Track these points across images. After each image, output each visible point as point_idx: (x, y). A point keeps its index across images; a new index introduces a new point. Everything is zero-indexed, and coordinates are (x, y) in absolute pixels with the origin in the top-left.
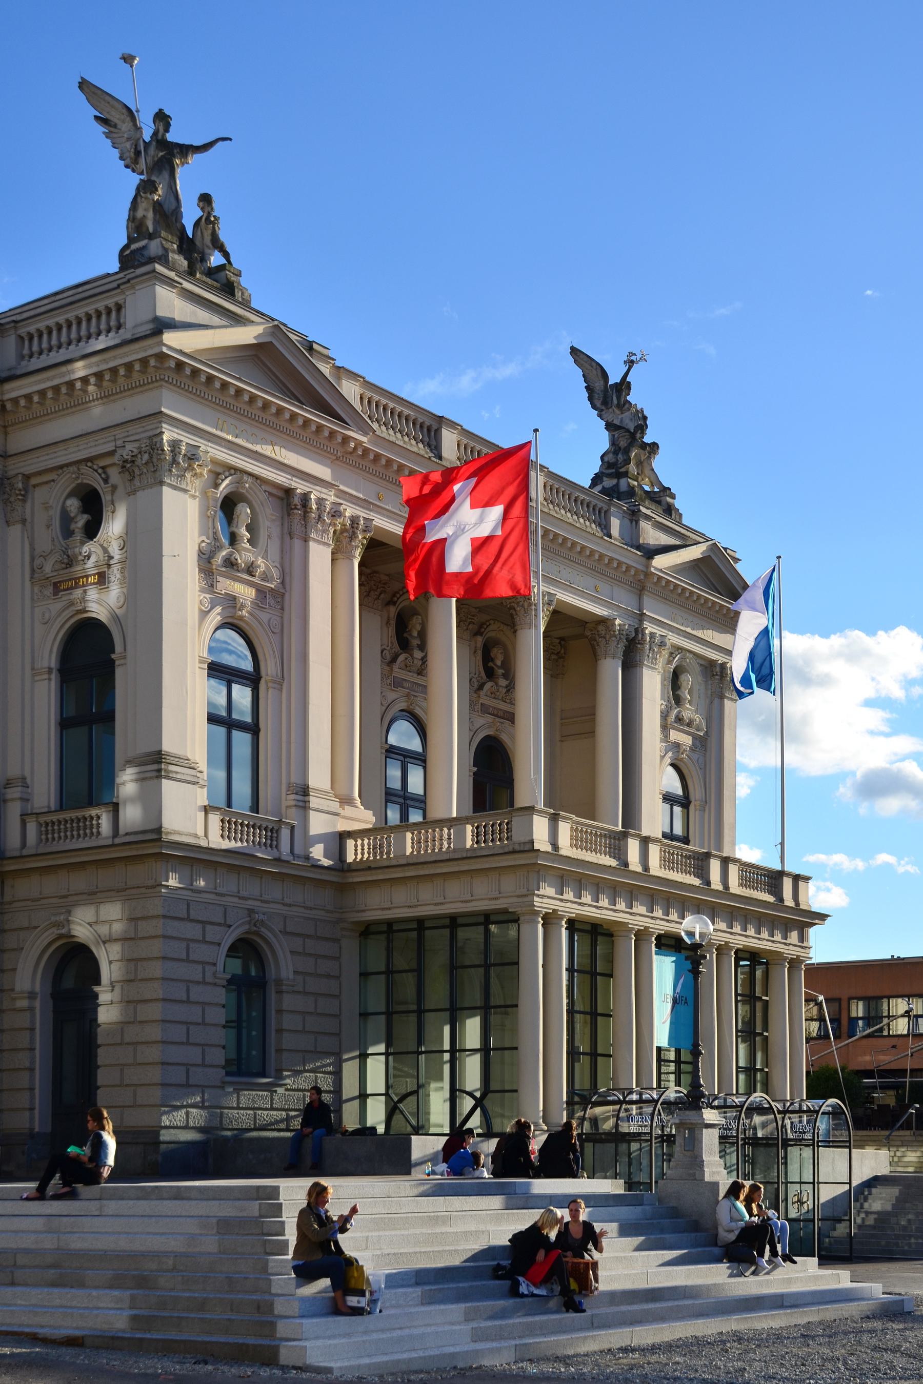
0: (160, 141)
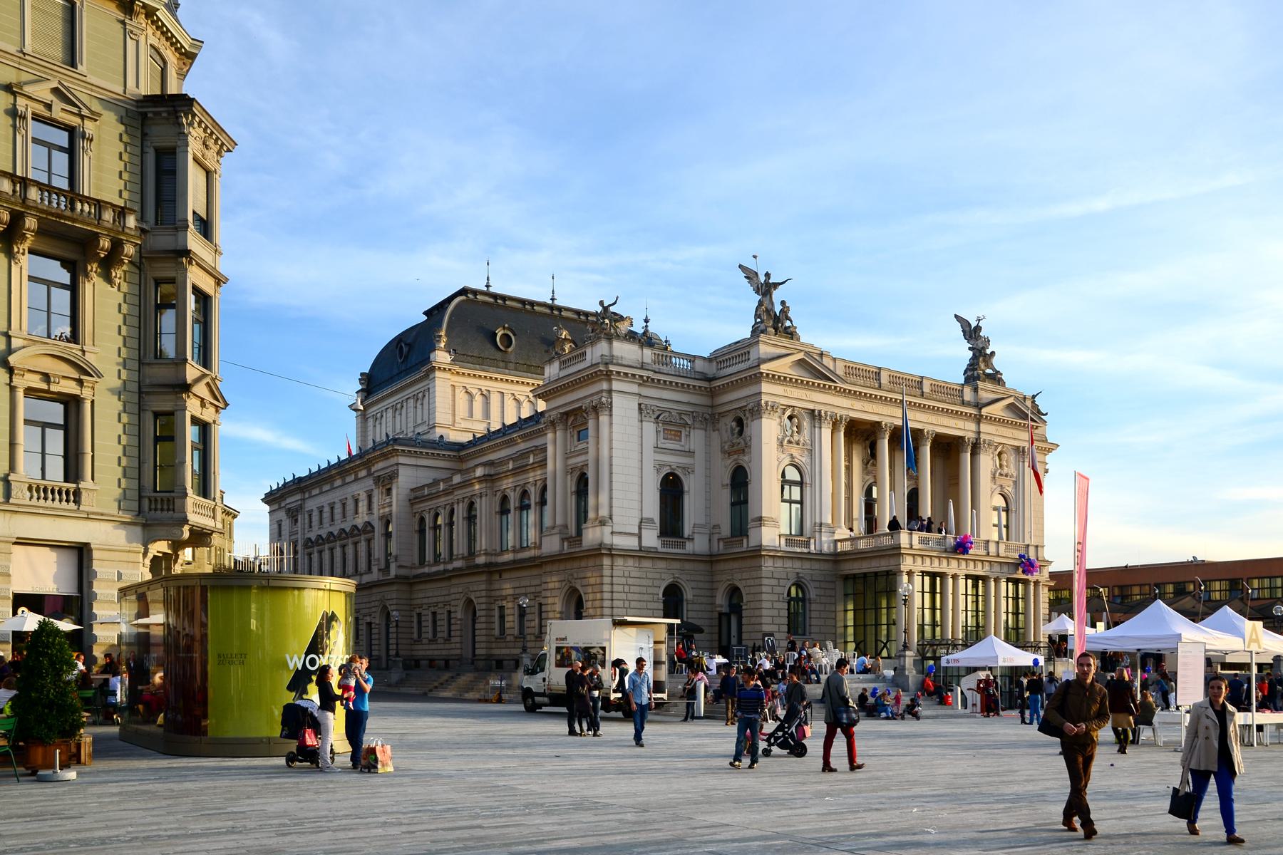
0: (767, 283)
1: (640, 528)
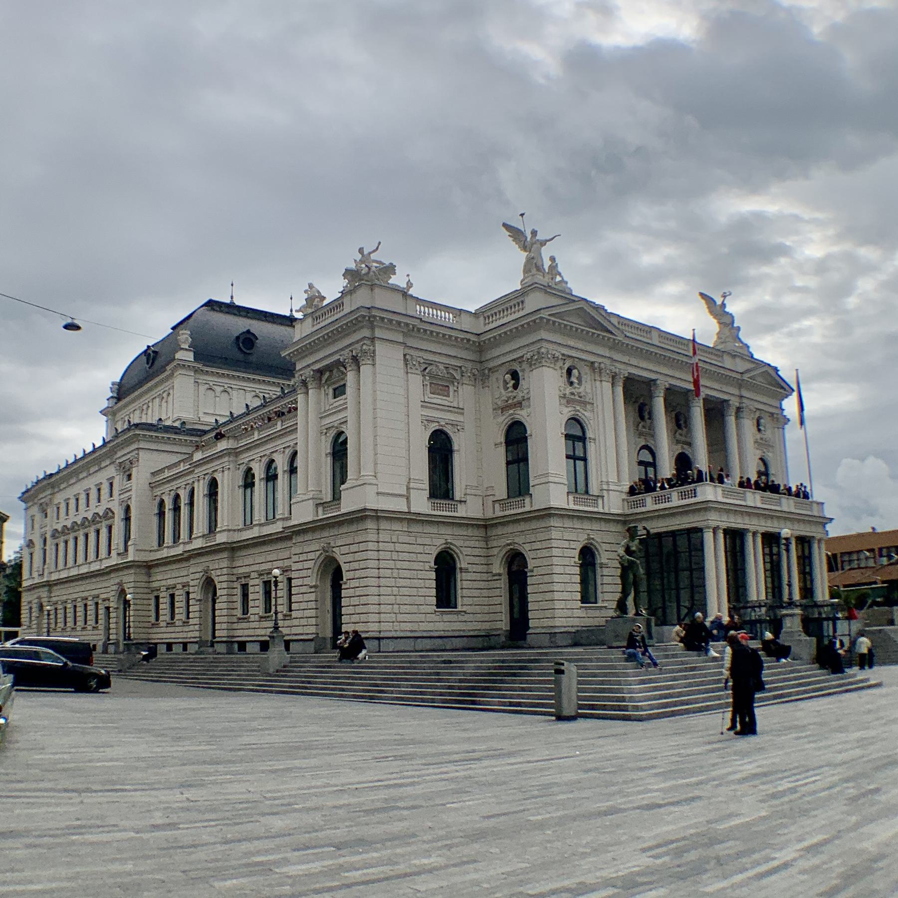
1: (408, 489)
